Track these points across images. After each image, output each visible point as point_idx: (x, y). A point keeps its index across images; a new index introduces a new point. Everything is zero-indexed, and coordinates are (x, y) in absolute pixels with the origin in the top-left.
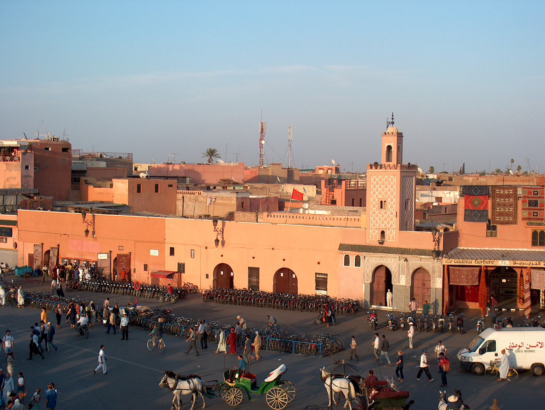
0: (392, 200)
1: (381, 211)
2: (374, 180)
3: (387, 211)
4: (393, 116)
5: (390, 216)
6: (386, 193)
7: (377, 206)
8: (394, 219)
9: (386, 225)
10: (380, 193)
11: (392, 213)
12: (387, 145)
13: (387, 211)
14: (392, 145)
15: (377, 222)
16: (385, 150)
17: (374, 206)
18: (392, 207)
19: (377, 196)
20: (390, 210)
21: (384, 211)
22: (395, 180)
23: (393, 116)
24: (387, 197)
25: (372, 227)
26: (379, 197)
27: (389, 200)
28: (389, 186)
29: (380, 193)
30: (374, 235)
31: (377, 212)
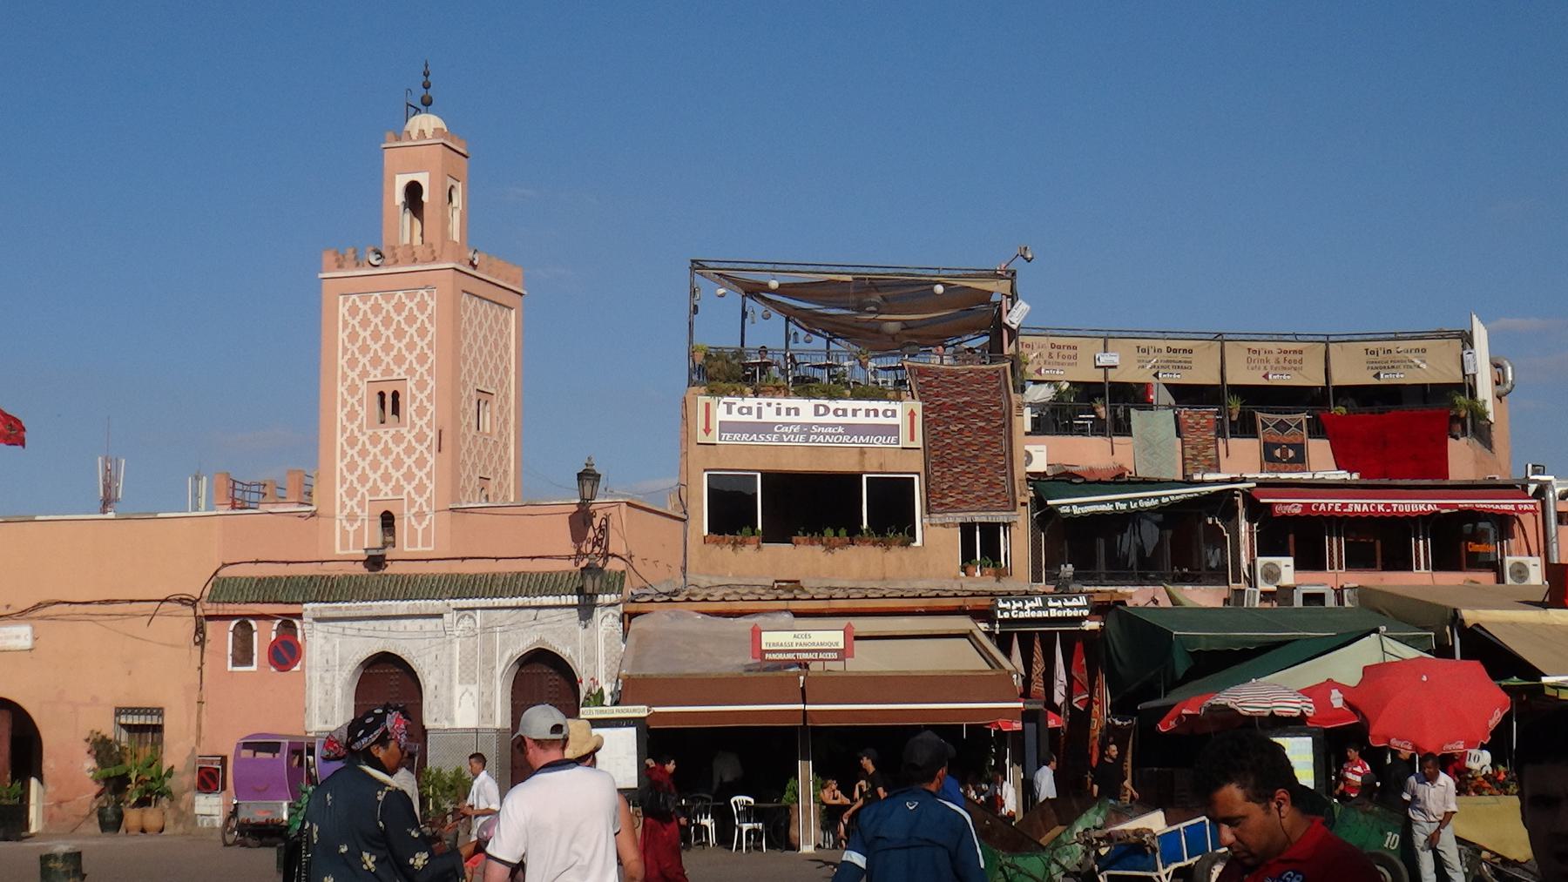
0: (421, 385)
1: (381, 432)
2: (354, 311)
3: (404, 430)
4: (426, 74)
5: (415, 449)
6: (399, 360)
7: (363, 413)
8: (431, 461)
9: (398, 489)
10: (376, 361)
11: (421, 438)
12: (401, 182)
13: (404, 430)
14: (423, 179)
15: (363, 479)
16: (399, 197)
17: (352, 416)
18: (421, 411)
19: (363, 374)
20: (413, 425)
21: (392, 431)
22: (432, 304)
23: (426, 74)
24: (403, 376)
25: (345, 499)
26: (371, 379)
27: (410, 384)
28: (412, 331)
29: (376, 361)
30: (351, 529)
31: (362, 438)
